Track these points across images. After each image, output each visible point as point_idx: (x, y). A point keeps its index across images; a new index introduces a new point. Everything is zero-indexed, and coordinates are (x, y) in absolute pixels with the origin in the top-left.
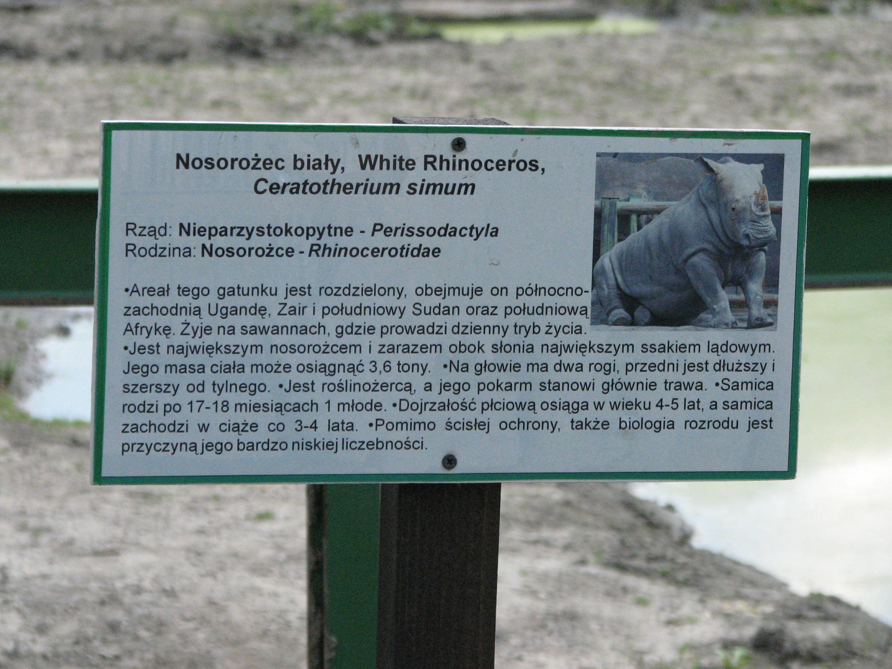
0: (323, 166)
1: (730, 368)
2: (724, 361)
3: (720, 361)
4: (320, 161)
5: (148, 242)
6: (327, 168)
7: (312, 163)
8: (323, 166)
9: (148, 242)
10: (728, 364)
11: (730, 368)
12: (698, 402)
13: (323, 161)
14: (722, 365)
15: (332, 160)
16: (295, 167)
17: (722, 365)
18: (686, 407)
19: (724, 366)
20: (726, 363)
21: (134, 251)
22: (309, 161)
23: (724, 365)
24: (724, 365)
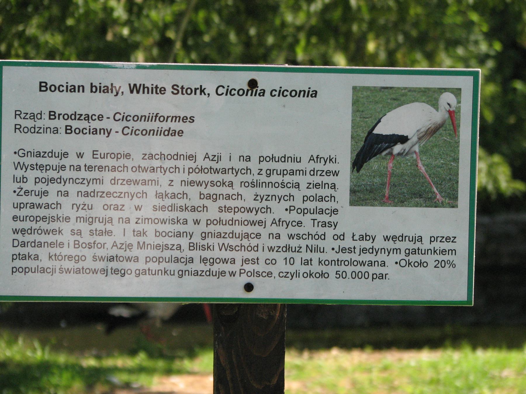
0: (110, 91)
1: (293, 250)
2: (289, 245)
3: (286, 245)
4: (108, 87)
5: (29, 123)
6: (112, 92)
7: (102, 89)
8: (110, 91)
9: (29, 123)
10: (292, 247)
11: (293, 250)
12: (311, 260)
13: (110, 87)
14: (288, 248)
15: (115, 87)
16: (92, 91)
17: (288, 248)
18: (303, 263)
19: (289, 249)
20: (290, 246)
21: (20, 129)
22: (100, 87)
23: (289, 248)
24: (289, 248)
